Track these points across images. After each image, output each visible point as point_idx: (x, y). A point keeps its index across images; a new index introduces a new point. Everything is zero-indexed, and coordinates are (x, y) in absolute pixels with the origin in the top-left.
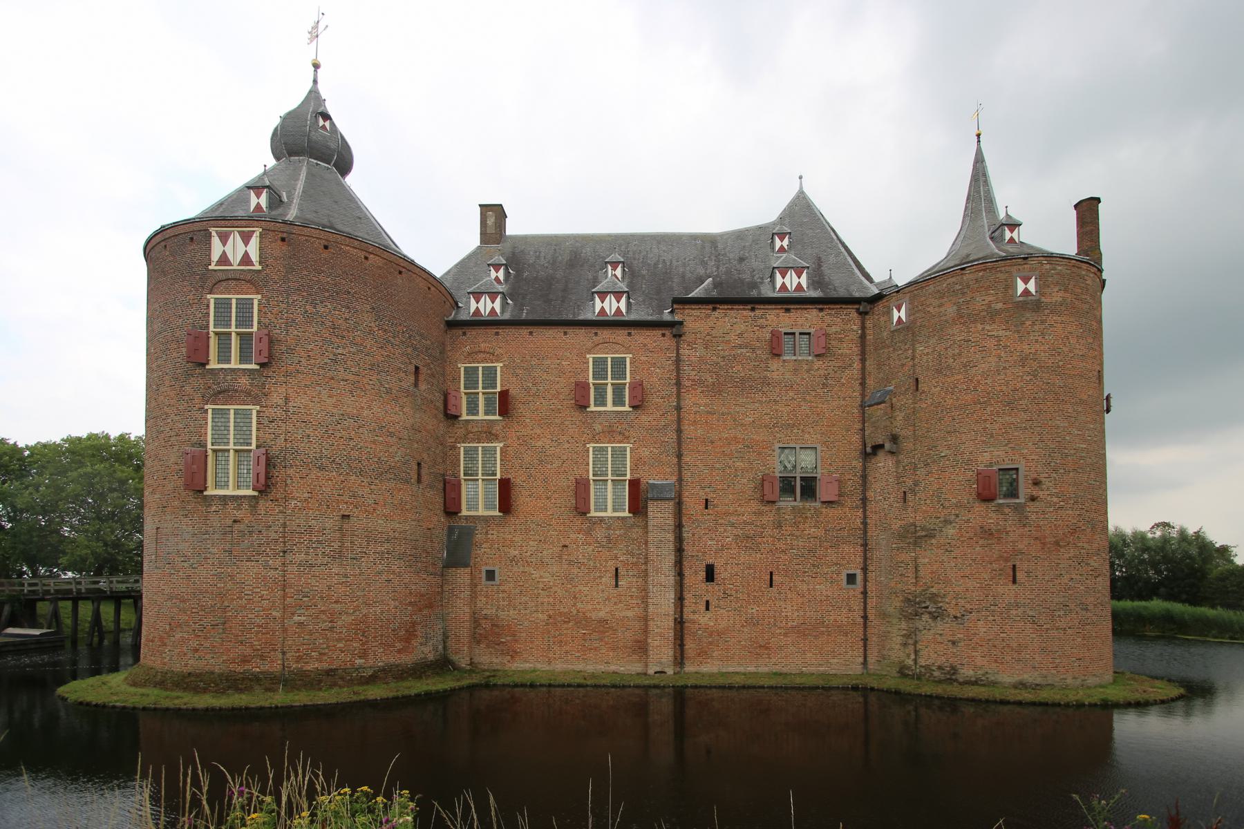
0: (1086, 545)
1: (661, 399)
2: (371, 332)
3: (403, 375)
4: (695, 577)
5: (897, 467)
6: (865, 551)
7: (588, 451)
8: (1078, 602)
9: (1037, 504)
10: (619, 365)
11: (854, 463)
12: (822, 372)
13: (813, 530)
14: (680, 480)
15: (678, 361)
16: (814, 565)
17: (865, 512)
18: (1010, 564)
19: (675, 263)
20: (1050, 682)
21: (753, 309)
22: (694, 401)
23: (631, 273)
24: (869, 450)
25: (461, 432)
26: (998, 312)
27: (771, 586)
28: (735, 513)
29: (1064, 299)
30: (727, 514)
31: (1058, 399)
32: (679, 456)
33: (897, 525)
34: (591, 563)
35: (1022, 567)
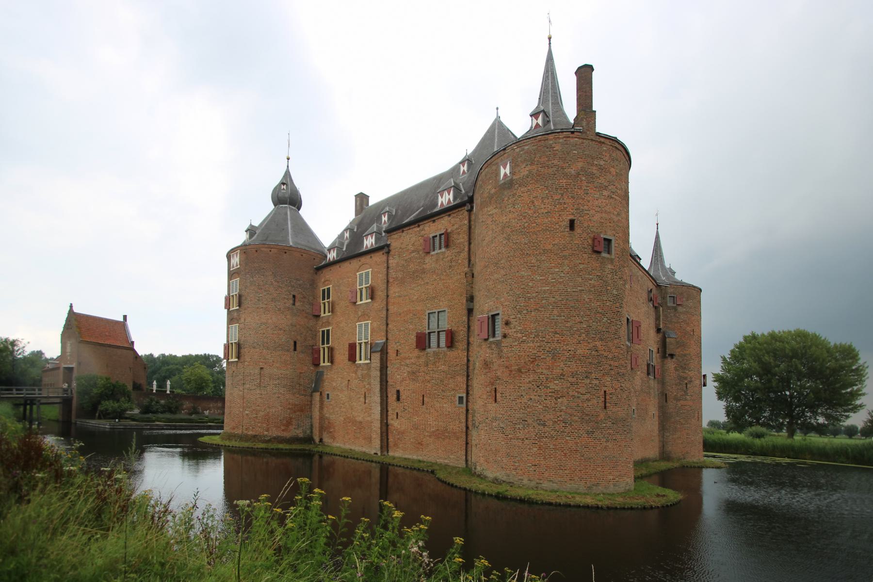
0: (545, 371)
2: (272, 284)
3: (286, 300)
6: (467, 380)
8: (536, 418)
13: (443, 366)
14: (387, 339)
16: (443, 391)
18: (494, 387)
20: (511, 481)
22: (394, 290)
31: (524, 254)
35: (499, 390)
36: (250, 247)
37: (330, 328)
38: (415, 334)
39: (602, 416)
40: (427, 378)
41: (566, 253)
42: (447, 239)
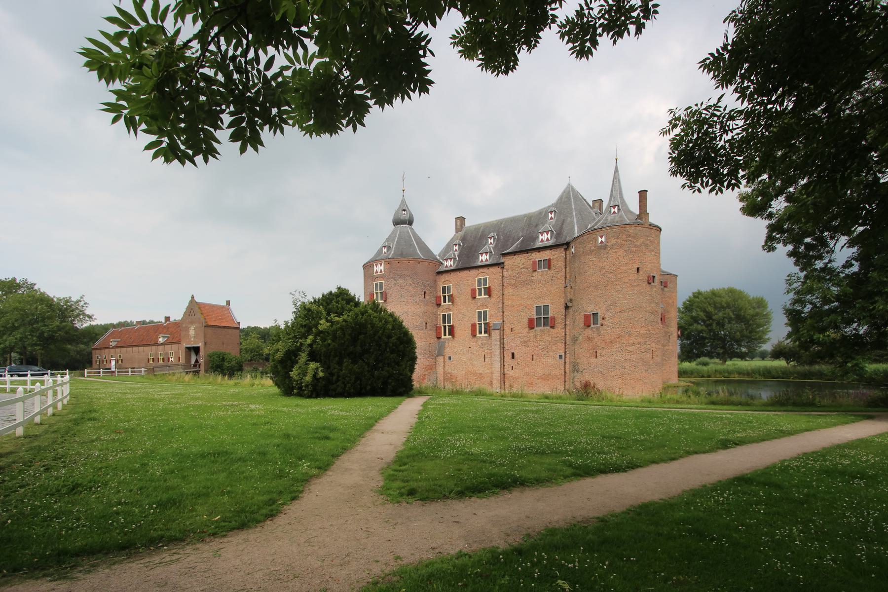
4: (508, 357)
6: (565, 346)
9: (604, 327)
14: (503, 321)
21: (527, 253)
29: (617, 242)
30: (519, 333)
36: (394, 260)
37: (451, 313)
38: (526, 318)
39: (651, 362)
40: (536, 344)
41: (635, 284)
42: (548, 264)
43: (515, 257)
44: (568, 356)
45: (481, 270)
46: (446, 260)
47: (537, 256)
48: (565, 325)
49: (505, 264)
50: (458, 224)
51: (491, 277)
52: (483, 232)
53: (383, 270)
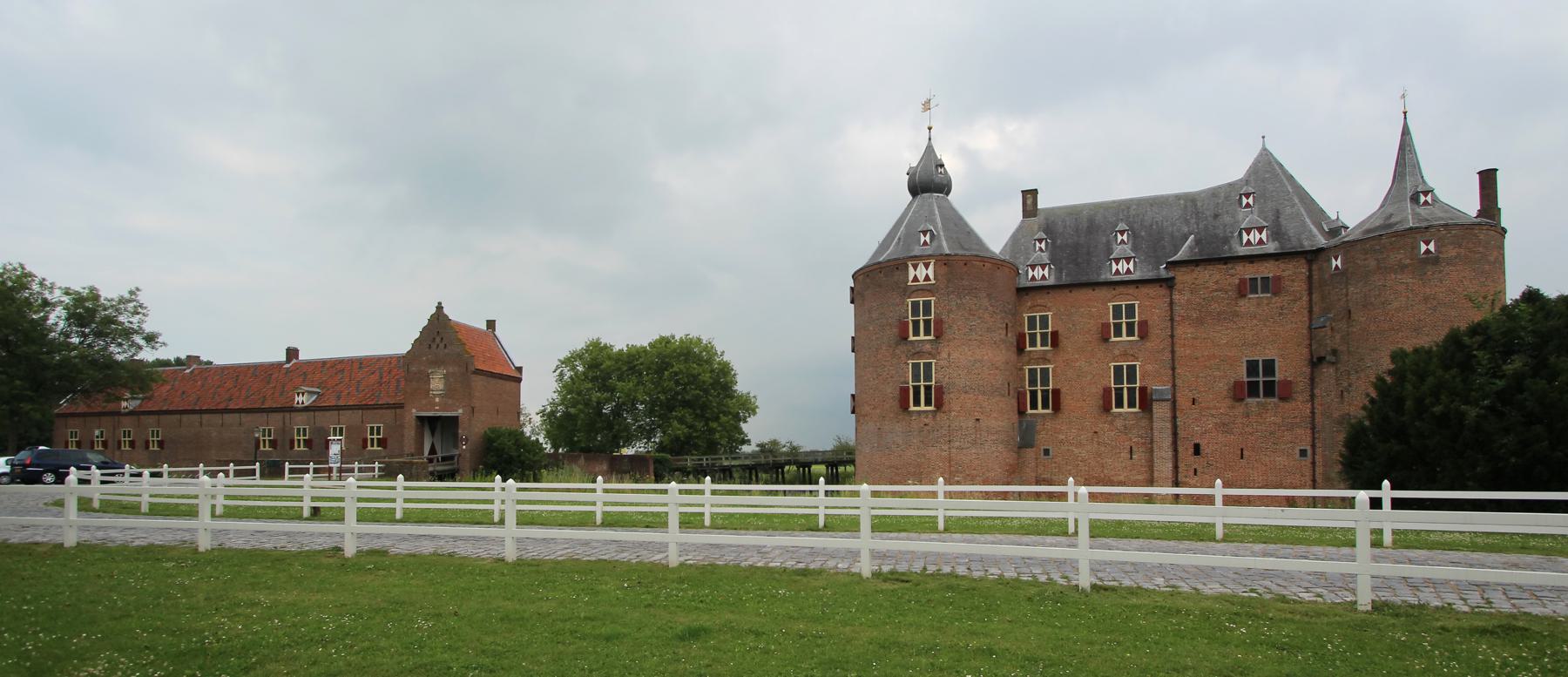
1: (1158, 330)
4: (1186, 452)
5: (1336, 373)
6: (1313, 433)
7: (1110, 368)
10: (1130, 309)
11: (1304, 369)
12: (1278, 305)
14: (1174, 386)
15: (1171, 303)
17: (1313, 405)
19: (1165, 224)
23: (1134, 236)
24: (1315, 360)
25: (1026, 359)
26: (1406, 266)
27: (1242, 458)
28: (1215, 408)
30: (1208, 408)
32: (1173, 369)
33: (1336, 415)
34: (1113, 443)
36: (956, 258)
43: (1198, 269)
44: (1319, 451)
45: (1121, 289)
46: (1033, 267)
47: (1249, 271)
48: (1312, 396)
49: (1176, 281)
50: (1029, 202)
51: (1146, 306)
52: (1091, 221)
53: (931, 277)
